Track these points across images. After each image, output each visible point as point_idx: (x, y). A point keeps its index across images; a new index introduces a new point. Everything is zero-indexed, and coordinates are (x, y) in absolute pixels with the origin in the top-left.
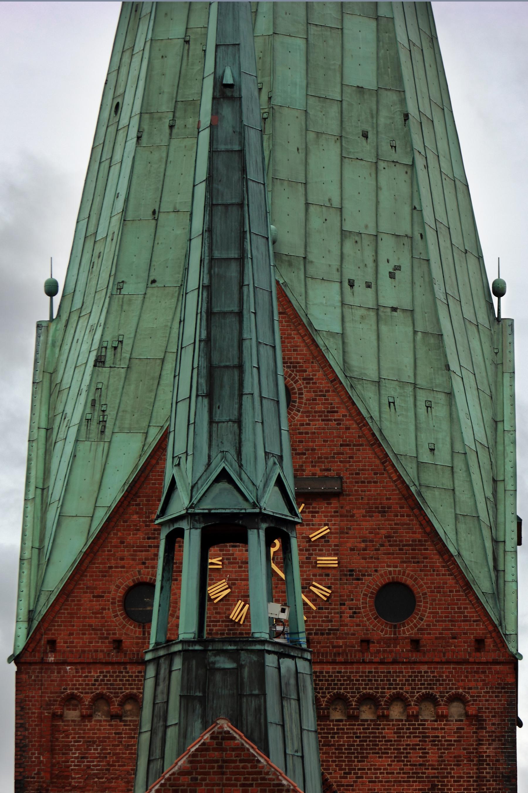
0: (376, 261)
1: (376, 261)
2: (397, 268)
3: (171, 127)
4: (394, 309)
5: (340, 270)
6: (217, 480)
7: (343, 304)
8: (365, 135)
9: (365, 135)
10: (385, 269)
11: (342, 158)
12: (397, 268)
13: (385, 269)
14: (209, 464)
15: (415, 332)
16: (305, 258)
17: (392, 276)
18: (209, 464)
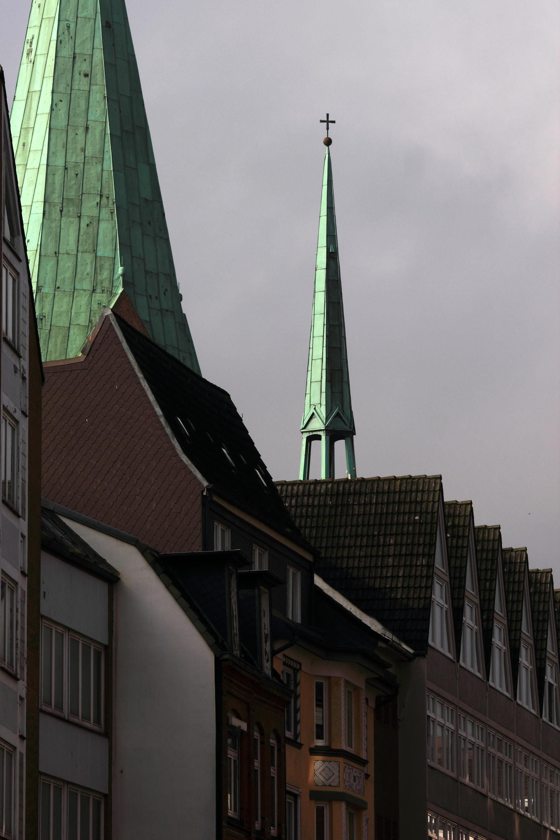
0: (158, 286)
1: (158, 286)
2: (166, 290)
3: (61, 211)
4: (167, 311)
5: (146, 290)
6: (335, 416)
7: (149, 307)
8: (150, 223)
9: (150, 223)
10: (162, 291)
11: (143, 234)
12: (166, 290)
13: (162, 291)
14: (332, 410)
15: (176, 322)
16: (133, 283)
17: (165, 294)
18: (332, 410)
